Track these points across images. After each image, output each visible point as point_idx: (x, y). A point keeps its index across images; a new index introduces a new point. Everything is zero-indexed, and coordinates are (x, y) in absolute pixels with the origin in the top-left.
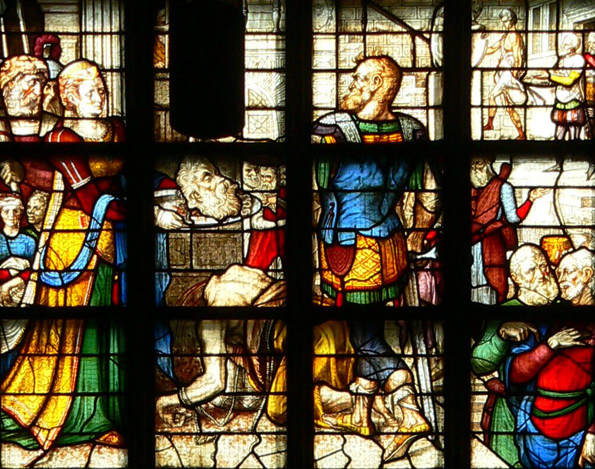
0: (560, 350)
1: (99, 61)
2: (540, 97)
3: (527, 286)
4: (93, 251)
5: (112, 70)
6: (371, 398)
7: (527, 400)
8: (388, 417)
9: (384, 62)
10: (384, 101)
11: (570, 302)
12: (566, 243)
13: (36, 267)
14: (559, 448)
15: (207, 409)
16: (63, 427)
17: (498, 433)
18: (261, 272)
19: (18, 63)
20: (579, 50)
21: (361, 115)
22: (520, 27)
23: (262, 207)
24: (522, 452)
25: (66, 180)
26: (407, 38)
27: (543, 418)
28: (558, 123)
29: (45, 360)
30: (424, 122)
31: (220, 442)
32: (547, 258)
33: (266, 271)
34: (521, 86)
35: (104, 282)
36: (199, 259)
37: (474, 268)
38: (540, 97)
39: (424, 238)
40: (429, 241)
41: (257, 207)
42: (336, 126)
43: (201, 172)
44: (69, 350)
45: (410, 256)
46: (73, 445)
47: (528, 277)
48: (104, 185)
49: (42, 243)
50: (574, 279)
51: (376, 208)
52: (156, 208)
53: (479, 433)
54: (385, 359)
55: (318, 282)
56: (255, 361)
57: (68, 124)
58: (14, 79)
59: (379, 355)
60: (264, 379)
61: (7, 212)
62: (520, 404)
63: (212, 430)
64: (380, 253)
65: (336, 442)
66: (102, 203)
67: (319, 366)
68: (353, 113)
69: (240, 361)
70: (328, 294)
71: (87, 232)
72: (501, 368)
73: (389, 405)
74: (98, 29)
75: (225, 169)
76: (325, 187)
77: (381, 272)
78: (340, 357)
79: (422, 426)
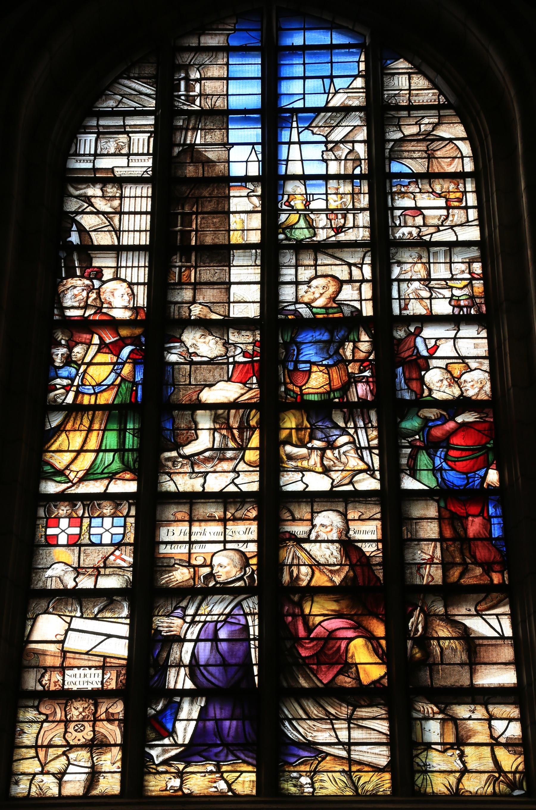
0: (464, 424)
1: (129, 280)
2: (440, 294)
3: (438, 389)
4: (119, 375)
5: (138, 284)
6: (323, 450)
7: (442, 451)
8: (336, 461)
9: (329, 279)
10: (330, 298)
11: (470, 398)
12: (465, 367)
13: (76, 383)
14: (468, 478)
15: (198, 459)
16: (88, 470)
17: (420, 470)
18: (241, 385)
19: (72, 281)
20: (467, 271)
21: (313, 305)
22: (424, 260)
23: (242, 351)
24: (440, 480)
25: (101, 338)
26: (346, 268)
27: (455, 461)
28: (454, 307)
29: (78, 433)
30: (359, 308)
31: (208, 477)
32: (452, 375)
33: (245, 384)
34: (427, 289)
35: (125, 390)
36: (195, 379)
37: (397, 380)
38: (440, 294)
39: (361, 365)
40: (365, 367)
41: (239, 351)
42: (296, 310)
43: (198, 334)
44: (96, 426)
45: (350, 376)
46: (96, 480)
47: (439, 384)
48: (129, 341)
49: (81, 370)
50: (473, 386)
51: (325, 350)
52: (166, 353)
53: (407, 470)
54: (332, 430)
55: (283, 389)
56: (235, 432)
57: (104, 310)
58: (68, 289)
59: (328, 428)
60: (242, 441)
61: (57, 355)
62: (436, 453)
63: (202, 470)
64: (329, 374)
65: (298, 476)
66: (126, 352)
67: (284, 434)
68: (308, 305)
69: (224, 432)
70: (290, 395)
71: (114, 364)
72: (421, 433)
73: (336, 454)
74: (130, 264)
75: (216, 333)
76: (288, 341)
77: (329, 384)
78: (298, 429)
79: (362, 466)
